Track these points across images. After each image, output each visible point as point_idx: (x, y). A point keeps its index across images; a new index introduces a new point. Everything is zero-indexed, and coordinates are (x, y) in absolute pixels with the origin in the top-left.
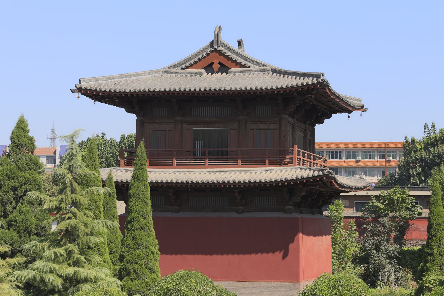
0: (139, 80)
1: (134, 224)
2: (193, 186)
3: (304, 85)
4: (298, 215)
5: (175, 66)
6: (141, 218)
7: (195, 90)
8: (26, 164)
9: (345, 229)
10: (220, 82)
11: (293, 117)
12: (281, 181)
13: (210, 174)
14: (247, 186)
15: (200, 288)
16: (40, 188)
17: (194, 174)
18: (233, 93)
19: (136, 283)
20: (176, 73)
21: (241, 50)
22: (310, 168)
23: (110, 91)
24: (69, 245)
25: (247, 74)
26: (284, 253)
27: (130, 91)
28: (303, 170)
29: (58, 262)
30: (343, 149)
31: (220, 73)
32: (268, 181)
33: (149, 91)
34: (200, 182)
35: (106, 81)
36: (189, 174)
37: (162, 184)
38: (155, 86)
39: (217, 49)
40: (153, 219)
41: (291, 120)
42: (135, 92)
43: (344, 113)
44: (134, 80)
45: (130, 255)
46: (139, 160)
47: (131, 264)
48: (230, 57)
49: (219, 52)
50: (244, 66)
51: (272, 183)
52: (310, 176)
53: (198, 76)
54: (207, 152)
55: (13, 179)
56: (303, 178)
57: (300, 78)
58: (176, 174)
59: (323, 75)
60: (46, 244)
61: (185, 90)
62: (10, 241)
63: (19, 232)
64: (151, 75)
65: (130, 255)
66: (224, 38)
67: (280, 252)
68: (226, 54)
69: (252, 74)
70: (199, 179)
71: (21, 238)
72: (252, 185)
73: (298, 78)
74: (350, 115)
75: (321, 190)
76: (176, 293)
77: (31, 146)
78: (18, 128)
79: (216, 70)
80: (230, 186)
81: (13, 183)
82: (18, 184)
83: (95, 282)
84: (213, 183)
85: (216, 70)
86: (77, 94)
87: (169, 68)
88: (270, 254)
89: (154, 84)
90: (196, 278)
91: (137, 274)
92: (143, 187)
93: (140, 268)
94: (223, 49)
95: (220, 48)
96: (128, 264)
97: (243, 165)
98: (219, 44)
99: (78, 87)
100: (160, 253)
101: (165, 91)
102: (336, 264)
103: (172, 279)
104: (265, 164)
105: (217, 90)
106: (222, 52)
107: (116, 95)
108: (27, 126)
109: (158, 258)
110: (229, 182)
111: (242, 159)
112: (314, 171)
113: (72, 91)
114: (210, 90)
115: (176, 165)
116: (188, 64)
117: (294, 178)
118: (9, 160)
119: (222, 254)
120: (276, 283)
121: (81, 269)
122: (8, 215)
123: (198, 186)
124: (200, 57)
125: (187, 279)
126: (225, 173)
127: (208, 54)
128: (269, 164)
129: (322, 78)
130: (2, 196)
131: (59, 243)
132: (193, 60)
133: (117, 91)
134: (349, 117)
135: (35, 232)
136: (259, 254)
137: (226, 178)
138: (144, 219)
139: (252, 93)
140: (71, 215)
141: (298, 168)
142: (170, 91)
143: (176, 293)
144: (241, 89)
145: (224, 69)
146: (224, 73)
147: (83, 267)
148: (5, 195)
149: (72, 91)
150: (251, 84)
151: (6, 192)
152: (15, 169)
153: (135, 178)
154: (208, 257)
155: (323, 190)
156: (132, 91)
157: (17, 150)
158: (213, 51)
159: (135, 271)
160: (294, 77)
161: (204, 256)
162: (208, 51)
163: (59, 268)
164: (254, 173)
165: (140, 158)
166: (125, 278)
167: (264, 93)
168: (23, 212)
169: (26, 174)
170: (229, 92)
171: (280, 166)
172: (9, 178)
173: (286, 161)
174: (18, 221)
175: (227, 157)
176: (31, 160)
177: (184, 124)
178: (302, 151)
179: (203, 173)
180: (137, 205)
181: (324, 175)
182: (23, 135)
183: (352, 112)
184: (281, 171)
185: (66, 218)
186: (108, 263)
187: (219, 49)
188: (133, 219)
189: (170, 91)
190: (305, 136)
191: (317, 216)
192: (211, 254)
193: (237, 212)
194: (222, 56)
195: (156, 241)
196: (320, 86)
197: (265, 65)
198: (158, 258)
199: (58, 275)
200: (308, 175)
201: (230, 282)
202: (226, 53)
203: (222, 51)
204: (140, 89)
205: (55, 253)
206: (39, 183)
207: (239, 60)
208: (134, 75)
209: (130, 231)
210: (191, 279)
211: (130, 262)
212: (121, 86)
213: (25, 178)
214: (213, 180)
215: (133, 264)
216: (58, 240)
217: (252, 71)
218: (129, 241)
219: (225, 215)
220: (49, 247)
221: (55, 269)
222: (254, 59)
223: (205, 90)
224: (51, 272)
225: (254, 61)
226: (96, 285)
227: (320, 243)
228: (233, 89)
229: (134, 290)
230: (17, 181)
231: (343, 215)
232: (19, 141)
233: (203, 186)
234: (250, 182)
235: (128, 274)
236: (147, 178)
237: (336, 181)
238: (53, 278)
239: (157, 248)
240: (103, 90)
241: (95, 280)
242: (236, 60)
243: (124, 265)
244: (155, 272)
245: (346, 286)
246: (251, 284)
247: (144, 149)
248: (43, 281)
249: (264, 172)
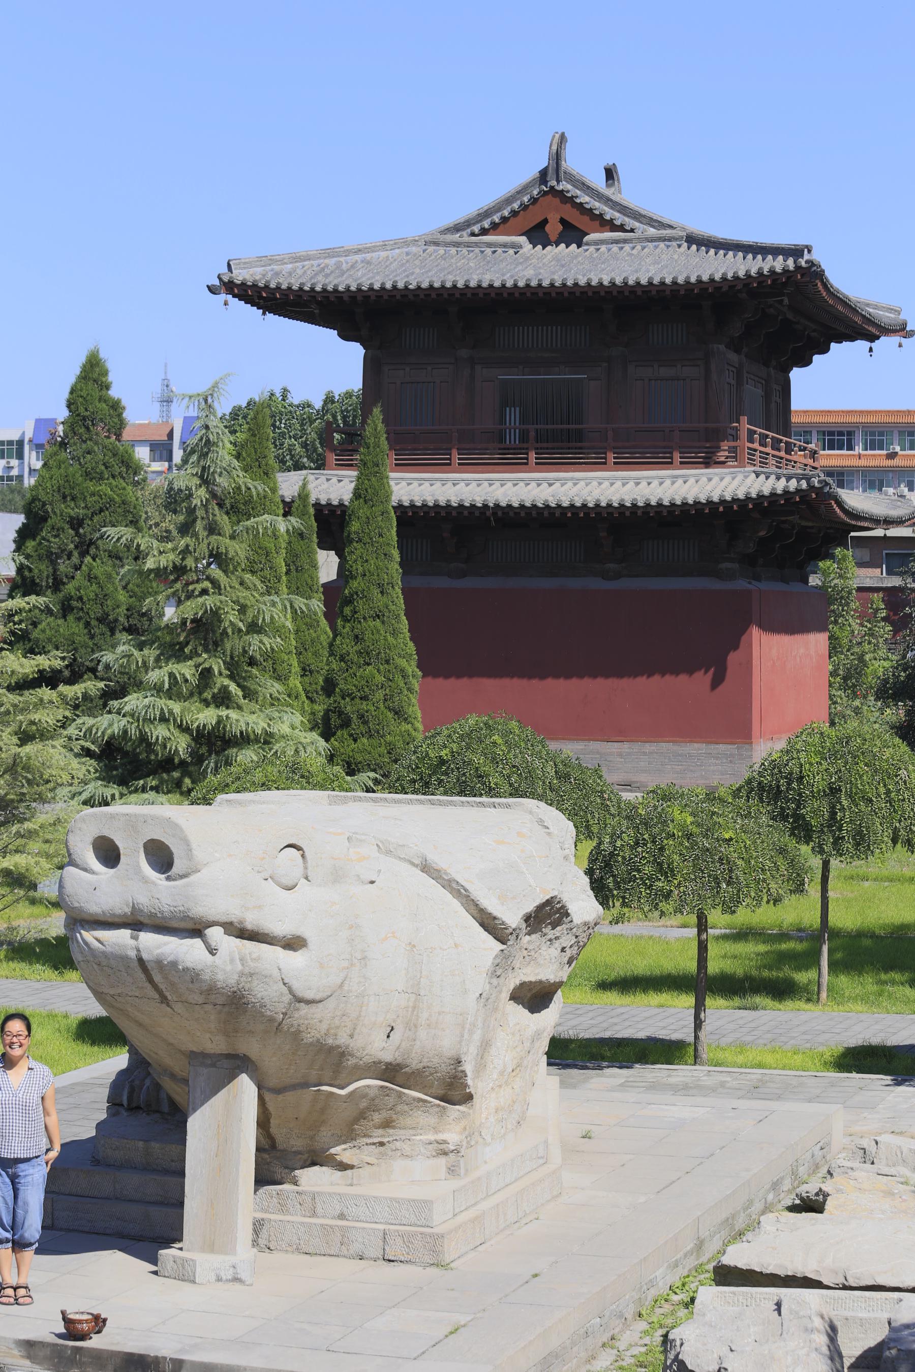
0: (369, 263)
1: (360, 605)
2: (500, 513)
3: (765, 273)
4: (750, 583)
5: (457, 228)
6: (376, 591)
7: (504, 286)
8: (104, 464)
9: (858, 617)
10: (563, 266)
11: (737, 351)
12: (710, 503)
13: (539, 485)
14: (628, 514)
15: (515, 756)
16: (137, 521)
17: (502, 485)
18: (594, 293)
19: (364, 745)
20: (457, 244)
21: (613, 189)
22: (779, 471)
23: (301, 289)
24: (205, 656)
25: (627, 247)
26: (714, 674)
27: (348, 289)
28: (762, 477)
29: (180, 697)
30: (857, 425)
31: (563, 245)
32: (679, 502)
33: (394, 287)
34: (516, 504)
35: (290, 266)
36: (490, 485)
37: (425, 509)
38: (407, 276)
39: (557, 188)
40: (403, 593)
41: (733, 357)
42: (359, 290)
43: (859, 341)
44: (357, 262)
45: (349, 679)
46: (369, 454)
47: (352, 699)
48: (588, 206)
49: (561, 195)
50: (621, 228)
51: (687, 508)
52: (779, 492)
53: (511, 251)
54: (532, 434)
55: (73, 499)
56: (760, 497)
57: (754, 258)
58: (458, 487)
59: (809, 251)
60: (151, 653)
61: (479, 286)
62: (69, 645)
63: (87, 624)
64: (397, 251)
65: (349, 679)
66: (572, 162)
67: (706, 672)
68: (578, 201)
69: (639, 247)
70: (514, 499)
71: (92, 637)
72: (639, 513)
73: (750, 256)
74: (873, 345)
75: (804, 523)
76: (458, 769)
77: (116, 420)
78: (84, 378)
79: (553, 237)
80: (587, 514)
81: (73, 509)
82: (85, 511)
83: (266, 742)
84: (547, 507)
85: (553, 237)
86: (223, 297)
88: (683, 677)
89: (405, 271)
90: (506, 734)
91: (366, 723)
92: (380, 519)
93: (373, 708)
94: (569, 187)
95: (564, 186)
96: (343, 698)
97: (620, 465)
98: (562, 175)
99: (226, 279)
100: (420, 673)
101: (431, 287)
102: (839, 700)
103: (450, 736)
104: (671, 463)
105: (557, 284)
106: (569, 195)
107: (314, 297)
108: (105, 373)
109: (416, 687)
110: (584, 506)
111: (615, 450)
112: (789, 479)
113: (212, 290)
114: (540, 285)
115: (459, 464)
116: (486, 224)
117: (741, 496)
118: (63, 455)
119: (568, 676)
121: (233, 714)
122: (64, 584)
123: (511, 514)
125: (485, 737)
126: (575, 484)
127: (534, 201)
128: (681, 463)
129: (806, 256)
130: (48, 541)
131: (182, 649)
132: (499, 215)
133: (318, 288)
134: (871, 350)
135: (126, 624)
136: (656, 678)
137: (577, 495)
138: (382, 593)
139: (639, 293)
140: (207, 584)
141: (749, 472)
142: (443, 287)
143: (458, 769)
144: (614, 284)
145: (572, 234)
146: (574, 246)
147: (240, 708)
148: (56, 536)
149: (212, 290)
150: (637, 271)
151: (58, 530)
152: (78, 475)
153: (360, 497)
154: (534, 682)
155: (810, 524)
156: (353, 288)
157: (82, 430)
158: (546, 193)
159: (363, 716)
160: (740, 254)
161: (524, 682)
162: (535, 192)
163: (182, 712)
164: (644, 483)
165: (371, 449)
166: (339, 733)
167: (668, 292)
168: (96, 578)
169: (104, 488)
170: (586, 290)
171: (706, 468)
172: (64, 497)
173: (722, 455)
174: (85, 599)
175: (579, 444)
176: (114, 455)
178: (759, 430)
179: (522, 484)
180: (367, 561)
181: (811, 487)
182: (97, 394)
183: (878, 338)
184: (710, 480)
185: (197, 593)
186: (296, 697)
187: (560, 188)
188: (357, 593)
189: (443, 287)
190: (767, 397)
191: (796, 587)
192: (543, 677)
193: (605, 576)
194: (568, 205)
195: (411, 645)
196: (802, 276)
197: (671, 227)
198: (416, 687)
199: (180, 726)
200: (773, 489)
201: (586, 743)
202: (576, 197)
203: (568, 192)
204: (371, 284)
205: (171, 675)
206: (135, 508)
207: (609, 213)
208: (359, 251)
209: (349, 621)
210: (496, 737)
211: (349, 695)
212: (327, 276)
213: (100, 496)
214: (547, 501)
215: (357, 701)
216: (178, 643)
217: (640, 240)
218: (346, 645)
219: (575, 583)
220: (157, 660)
221: (171, 712)
222: (643, 212)
223: (528, 286)
224: (163, 719)
225: (644, 216)
226: (270, 750)
227: (802, 651)
228: (593, 284)
229: (360, 762)
230: (83, 505)
231: (855, 584)
232: (86, 410)
233: (523, 514)
234: (634, 505)
235: (346, 723)
236: (388, 496)
237: (840, 504)
238: (168, 734)
239: (414, 663)
240: (284, 287)
241: (267, 739)
242: (601, 215)
243: (335, 701)
244: (410, 719)
245: (863, 753)
246: (636, 747)
247: (381, 426)
248: (143, 738)
249: (668, 482)
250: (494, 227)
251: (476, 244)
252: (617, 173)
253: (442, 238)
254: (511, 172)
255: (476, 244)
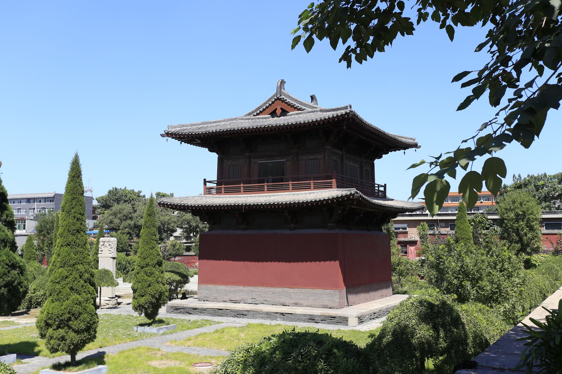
5: (249, 114)
11: (341, 150)
20: (249, 119)
25: (301, 115)
41: (340, 152)
50: (299, 110)
79: (278, 115)
85: (278, 115)
86: (166, 138)
87: (245, 116)
95: (282, 97)
116: (258, 112)
120: (319, 290)
124: (267, 105)
127: (273, 102)
145: (284, 113)
158: (276, 100)
177: (252, 159)
181: (351, 194)
193: (291, 229)
207: (297, 105)
208: (215, 122)
217: (305, 113)
219: (279, 232)
246: (299, 290)
250: (261, 112)
251: (254, 119)
252: (315, 98)
253: (244, 117)
254: (265, 94)
255: (254, 119)
